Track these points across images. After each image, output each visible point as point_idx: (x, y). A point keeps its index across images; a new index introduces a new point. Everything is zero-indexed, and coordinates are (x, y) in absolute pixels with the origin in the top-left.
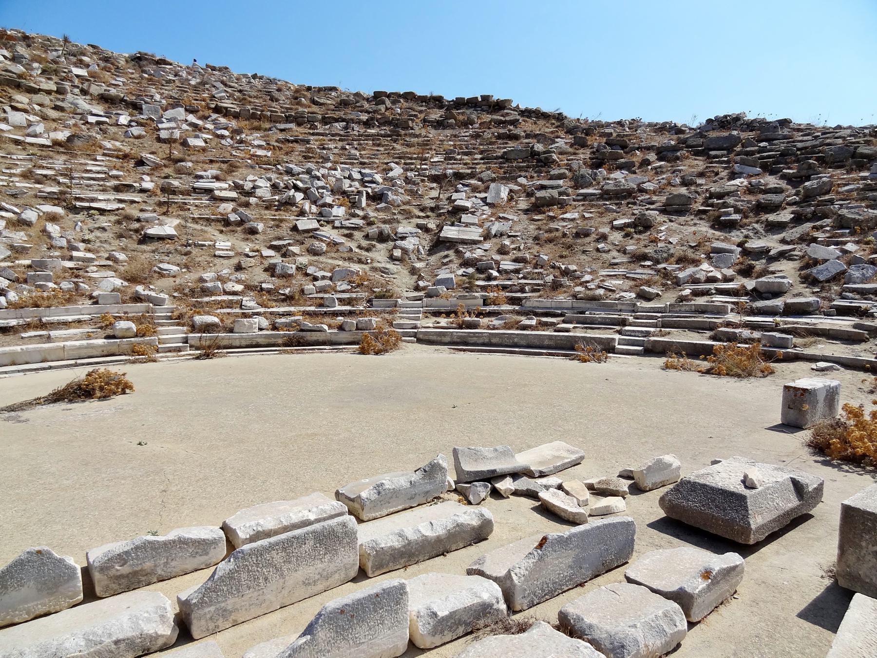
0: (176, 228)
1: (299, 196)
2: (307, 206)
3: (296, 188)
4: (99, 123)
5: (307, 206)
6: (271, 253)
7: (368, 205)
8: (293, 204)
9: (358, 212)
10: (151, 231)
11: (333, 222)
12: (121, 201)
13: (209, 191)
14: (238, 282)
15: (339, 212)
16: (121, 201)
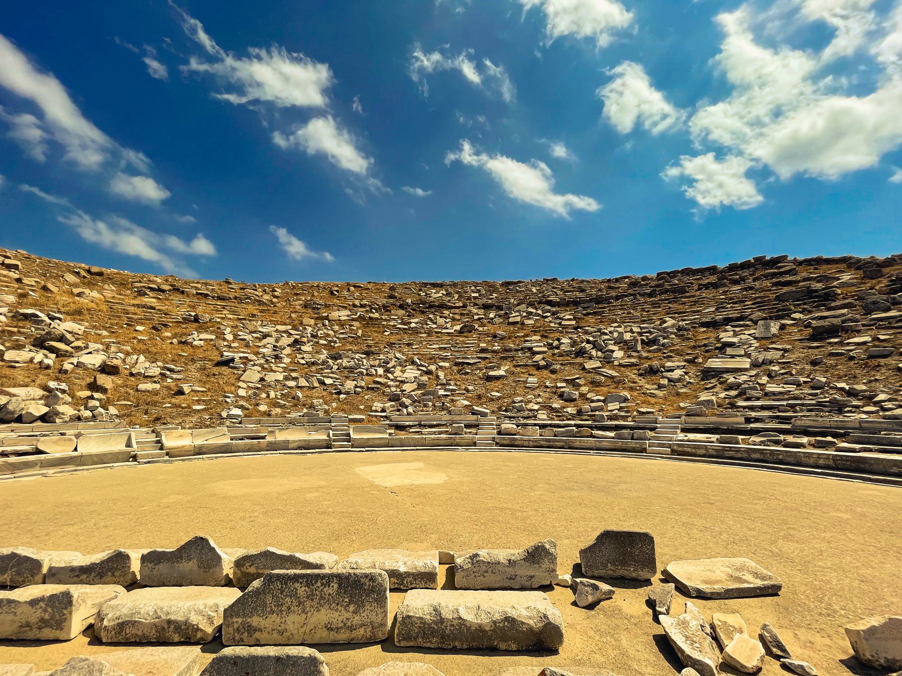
0: (505, 371)
1: (588, 347)
2: (594, 352)
3: (588, 342)
4: (479, 319)
5: (594, 352)
6: (564, 385)
7: (643, 348)
8: (585, 353)
9: (634, 354)
10: (491, 373)
11: (613, 362)
12: (479, 358)
13: (530, 349)
14: (537, 403)
15: (618, 354)
16: (479, 358)
